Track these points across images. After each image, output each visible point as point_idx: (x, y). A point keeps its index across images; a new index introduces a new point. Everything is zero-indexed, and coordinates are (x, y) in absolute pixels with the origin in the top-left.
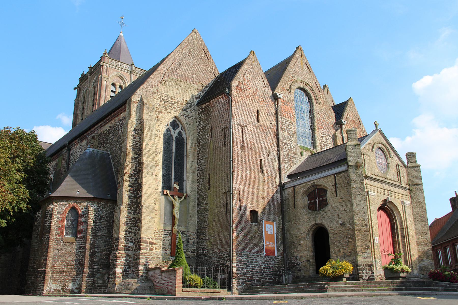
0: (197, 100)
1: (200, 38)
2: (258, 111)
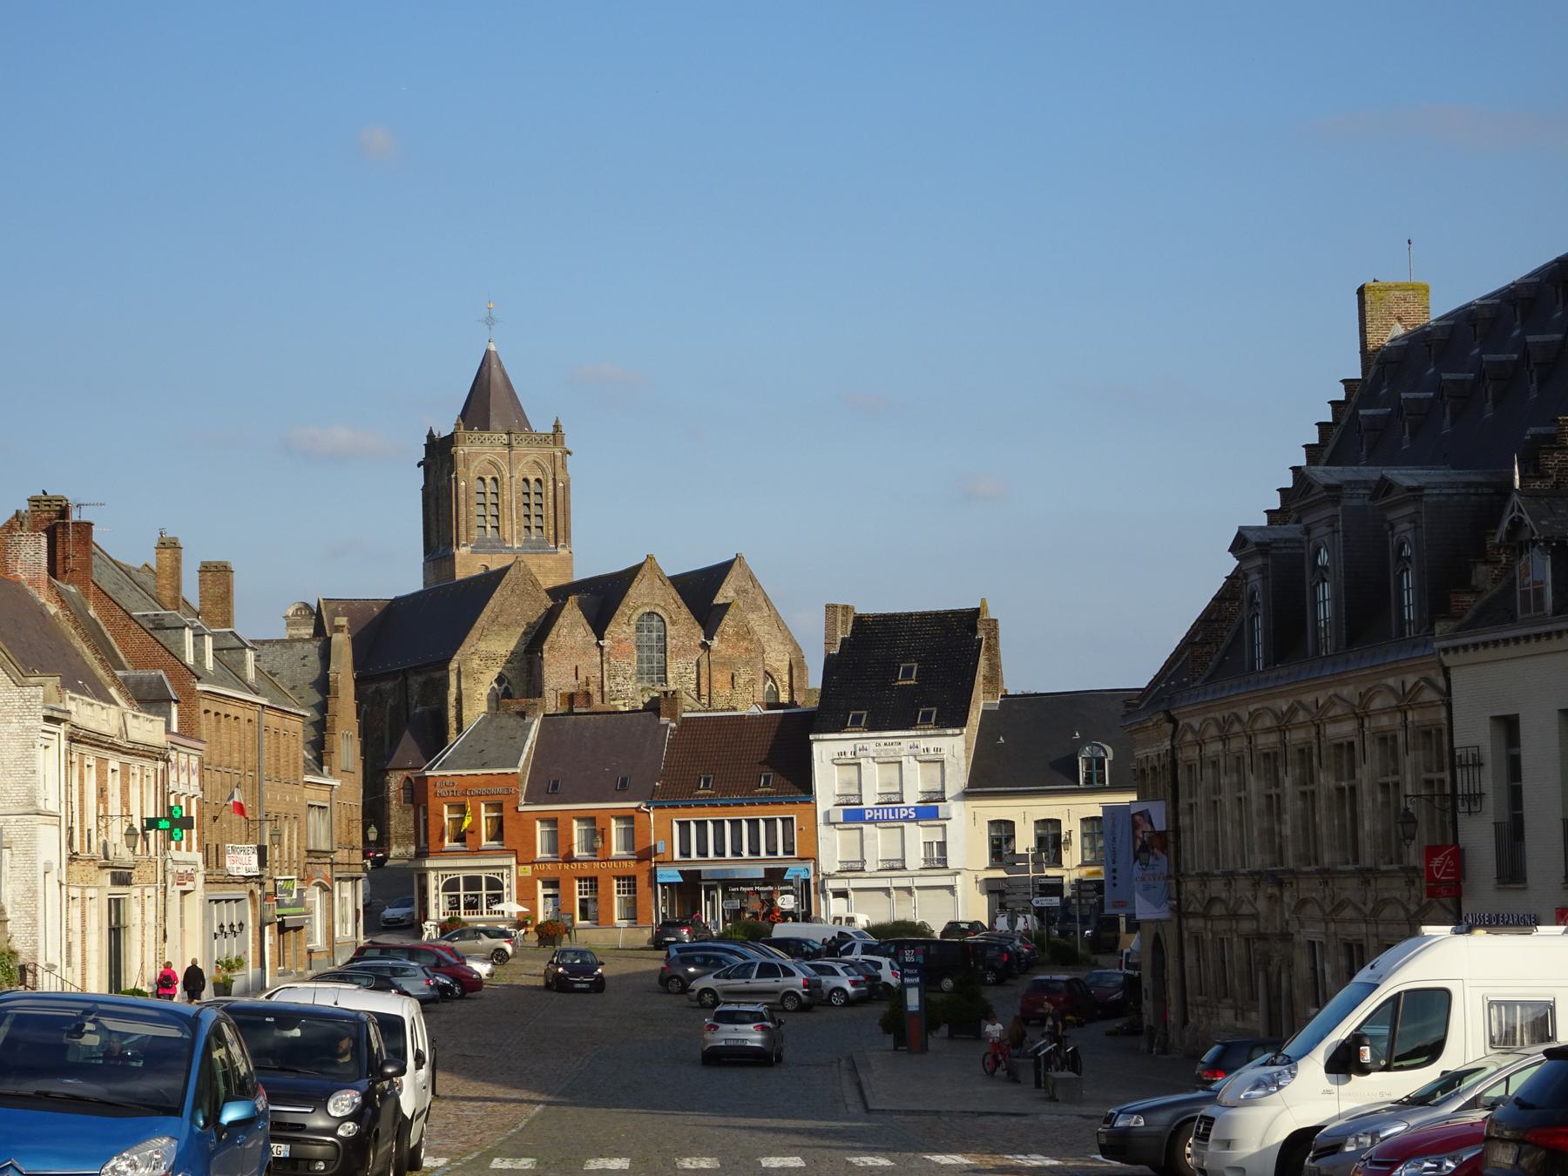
0: (524, 646)
1: (525, 566)
2: (577, 667)
